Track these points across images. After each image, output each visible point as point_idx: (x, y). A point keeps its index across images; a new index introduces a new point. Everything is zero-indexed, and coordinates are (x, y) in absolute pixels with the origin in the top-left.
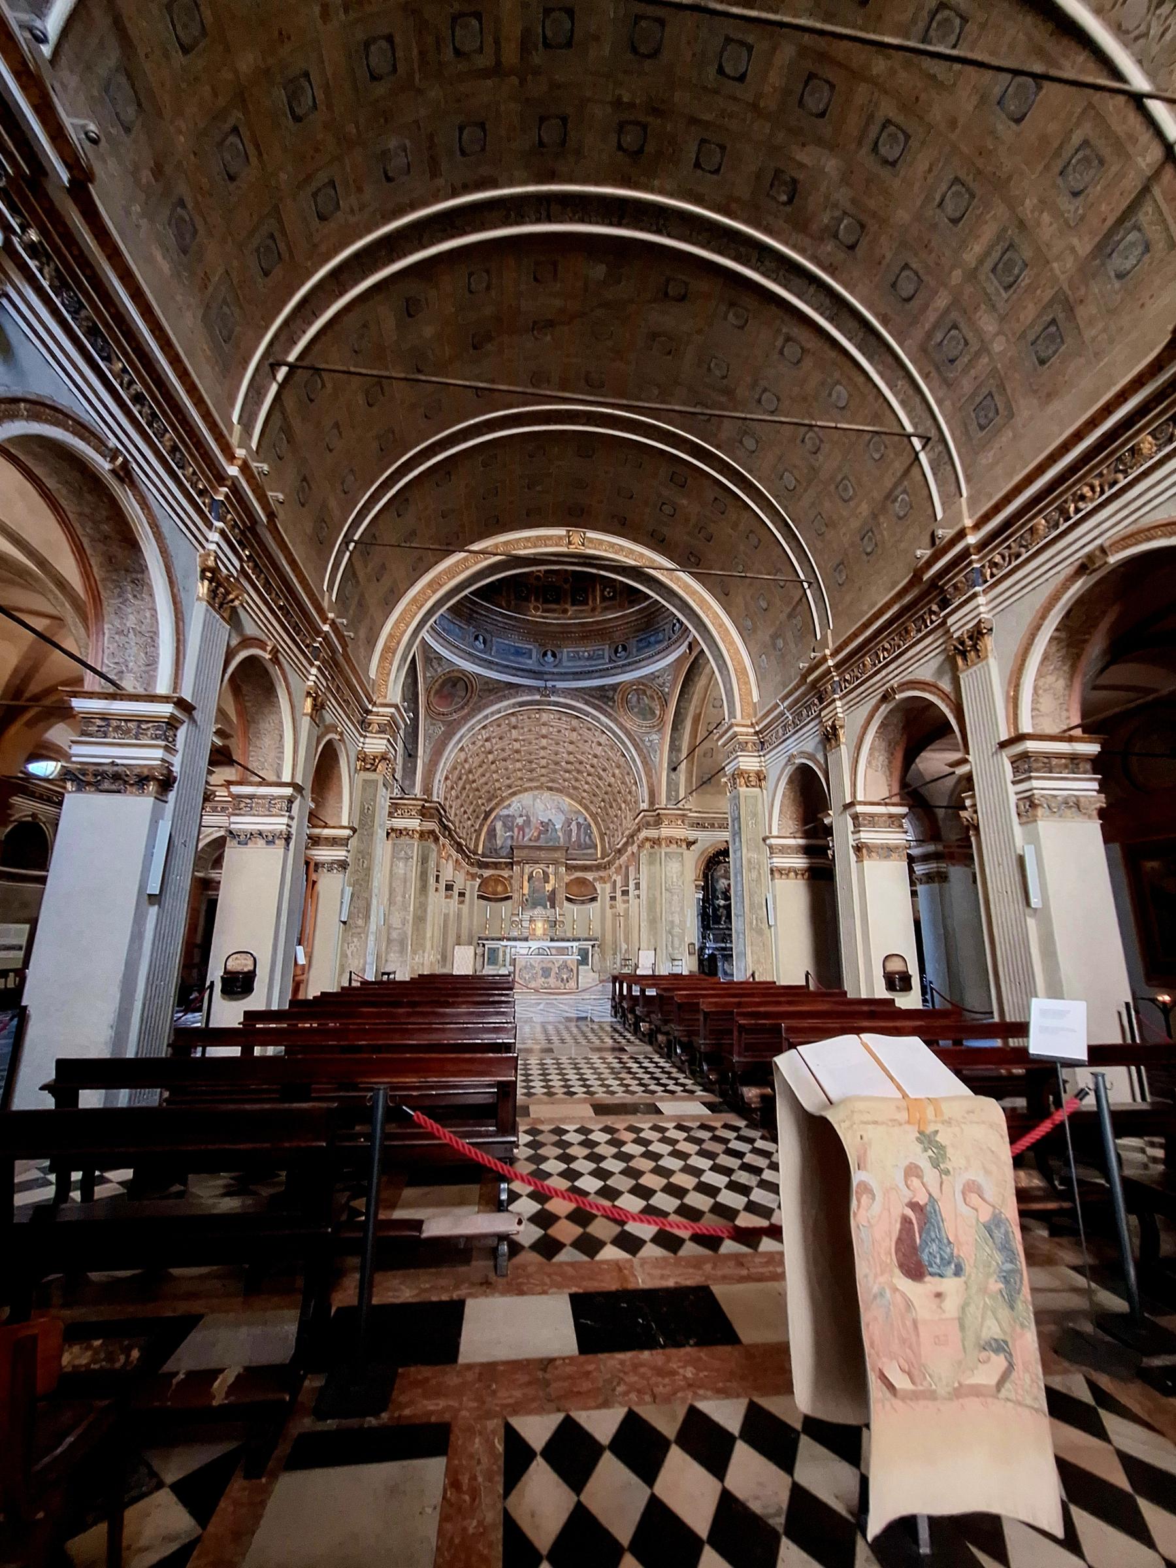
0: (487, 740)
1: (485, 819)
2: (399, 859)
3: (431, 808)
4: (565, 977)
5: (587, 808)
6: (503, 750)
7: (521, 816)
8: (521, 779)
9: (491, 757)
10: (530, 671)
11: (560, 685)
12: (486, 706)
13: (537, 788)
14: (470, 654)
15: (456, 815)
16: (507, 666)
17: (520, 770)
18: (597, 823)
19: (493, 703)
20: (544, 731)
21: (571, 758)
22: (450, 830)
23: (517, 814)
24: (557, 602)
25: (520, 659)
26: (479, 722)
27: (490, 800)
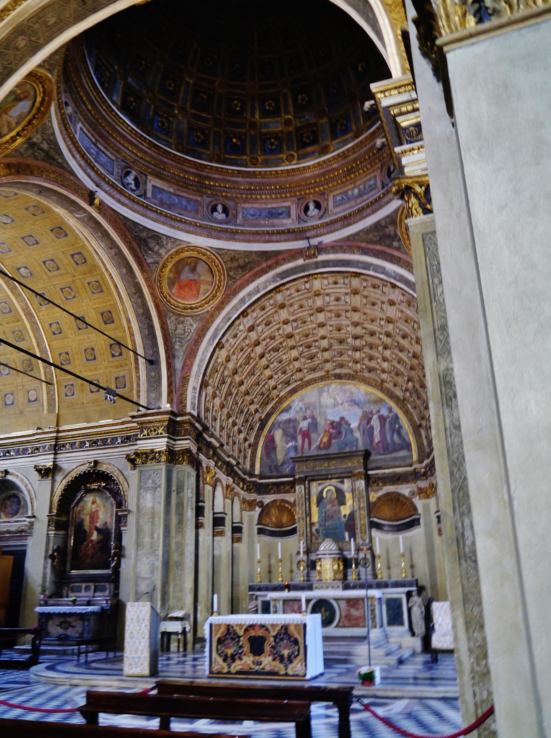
0: (251, 329)
1: (261, 429)
2: (147, 489)
3: (183, 422)
4: (286, 652)
5: (392, 396)
6: (273, 338)
7: (305, 418)
8: (300, 370)
9: (259, 350)
10: (289, 231)
11: (328, 239)
12: (242, 287)
13: (322, 378)
14: (201, 226)
15: (222, 428)
16: (257, 233)
17: (296, 359)
18: (407, 413)
19: (249, 282)
20: (319, 302)
21: (359, 331)
22: (214, 448)
23: (299, 417)
24: (315, 142)
25: (276, 221)
26: (235, 308)
27: (265, 404)
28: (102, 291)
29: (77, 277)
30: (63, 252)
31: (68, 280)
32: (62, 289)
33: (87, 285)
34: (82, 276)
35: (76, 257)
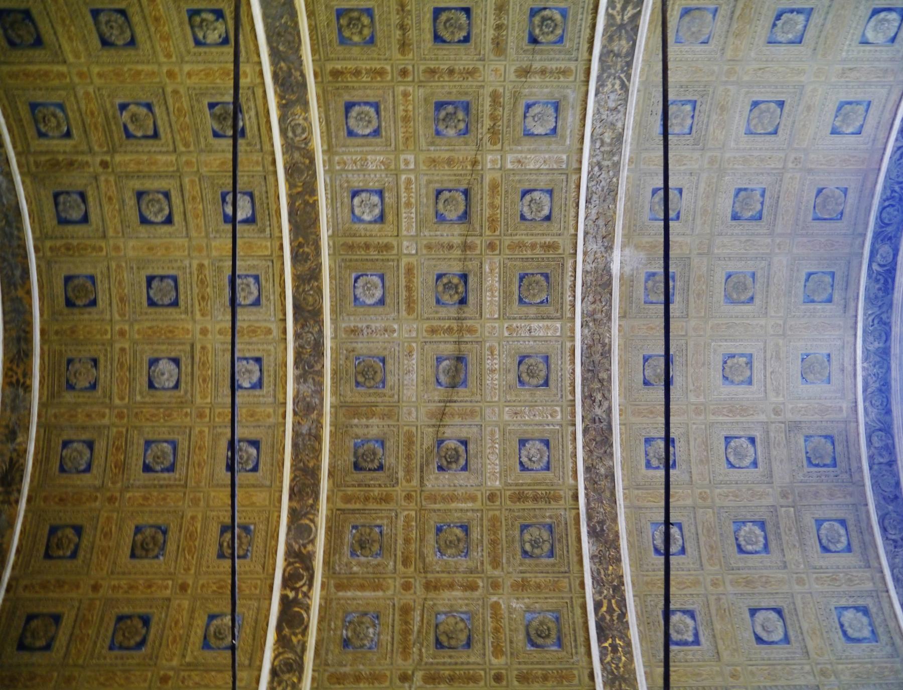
28: (33, 106)
29: (98, 160)
30: (104, 237)
31: (127, 158)
32: (156, 135)
33: (74, 132)
34: (80, 158)
35: (76, 215)
